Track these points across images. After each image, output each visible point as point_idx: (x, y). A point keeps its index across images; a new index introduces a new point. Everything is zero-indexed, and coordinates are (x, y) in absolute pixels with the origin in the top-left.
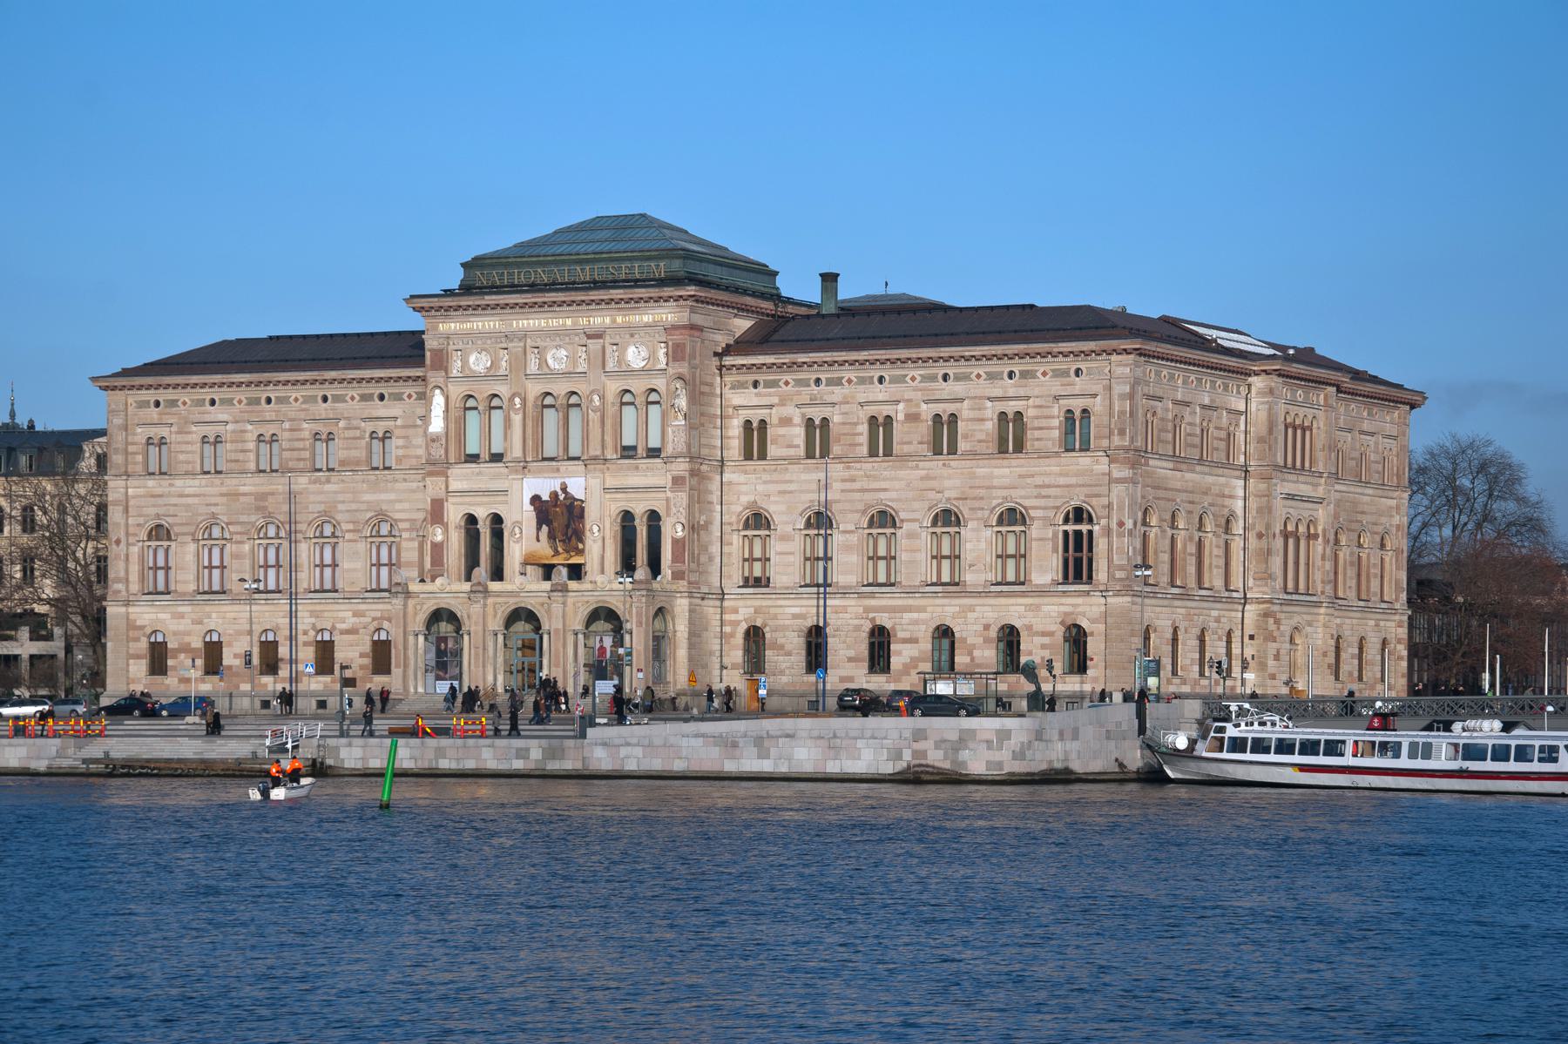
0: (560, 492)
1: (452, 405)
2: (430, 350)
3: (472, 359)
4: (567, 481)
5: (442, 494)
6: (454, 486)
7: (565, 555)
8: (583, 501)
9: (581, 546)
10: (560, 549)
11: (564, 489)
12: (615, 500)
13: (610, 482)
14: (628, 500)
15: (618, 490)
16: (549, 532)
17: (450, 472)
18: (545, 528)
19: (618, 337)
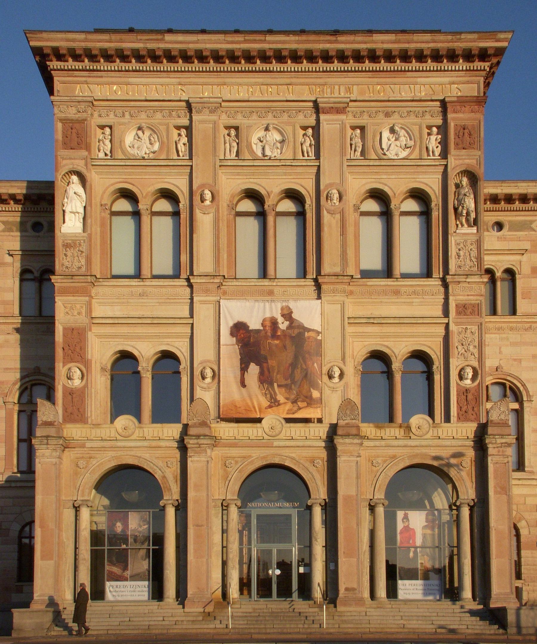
0: (280, 319)
1: (97, 201)
2: (61, 120)
3: (129, 138)
4: (292, 305)
5: (82, 320)
6: (99, 311)
7: (289, 406)
8: (318, 333)
9: (315, 394)
10: (281, 398)
11: (288, 315)
12: (363, 335)
13: (351, 311)
14: (383, 336)
15: (371, 321)
16: (262, 373)
17: (94, 291)
18: (254, 369)
19: (366, 116)
